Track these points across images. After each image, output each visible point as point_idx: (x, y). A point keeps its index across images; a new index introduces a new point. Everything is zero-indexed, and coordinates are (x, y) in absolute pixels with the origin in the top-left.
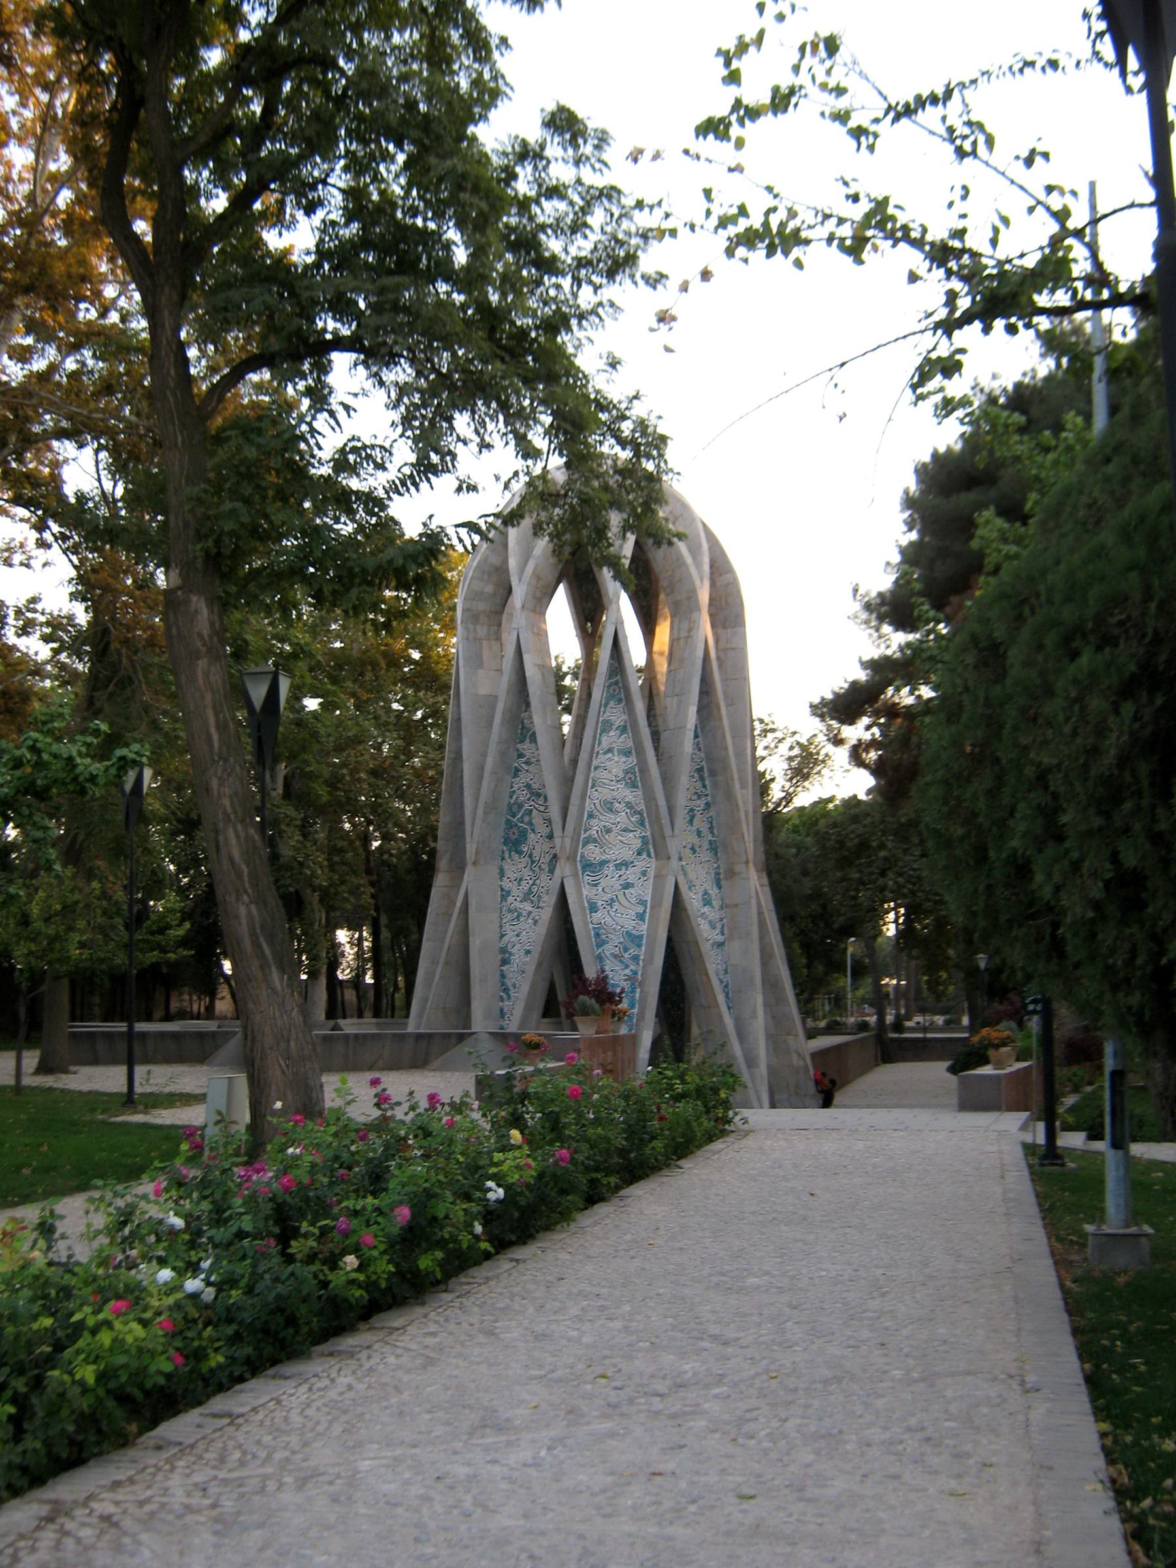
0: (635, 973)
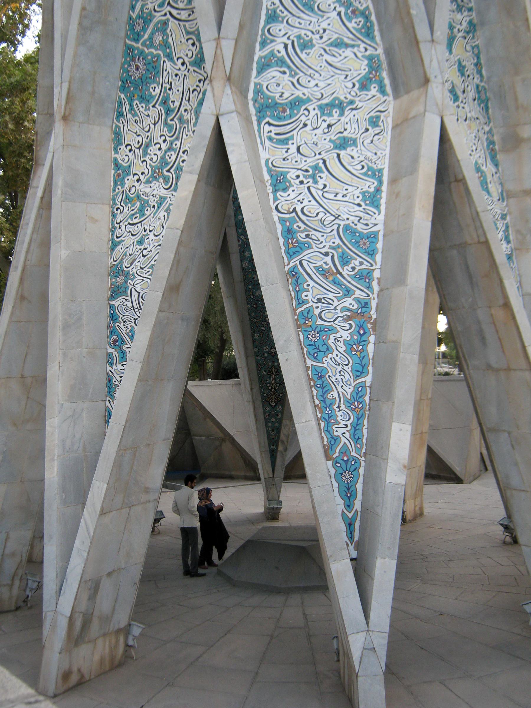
0: (366, 305)
